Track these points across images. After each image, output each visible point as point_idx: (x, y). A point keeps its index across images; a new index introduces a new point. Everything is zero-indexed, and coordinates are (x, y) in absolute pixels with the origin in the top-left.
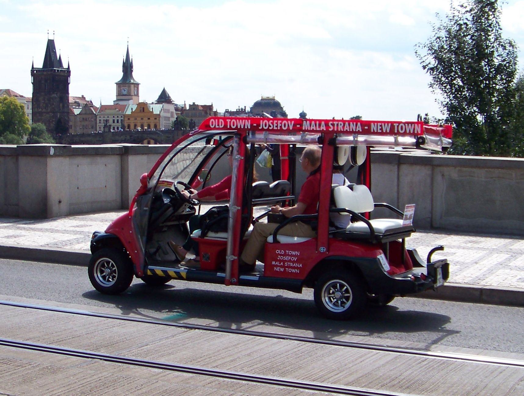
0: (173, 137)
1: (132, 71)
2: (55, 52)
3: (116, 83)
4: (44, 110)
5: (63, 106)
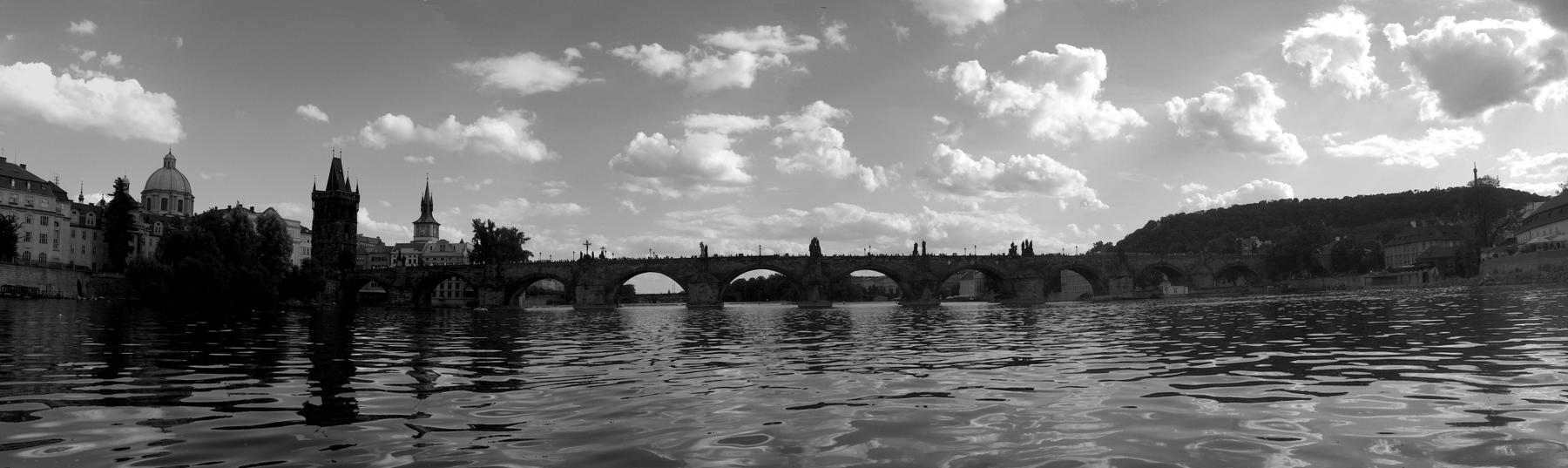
0: (485, 274)
1: (431, 210)
2: (342, 173)
3: (414, 223)
4: (326, 241)
5: (349, 238)
